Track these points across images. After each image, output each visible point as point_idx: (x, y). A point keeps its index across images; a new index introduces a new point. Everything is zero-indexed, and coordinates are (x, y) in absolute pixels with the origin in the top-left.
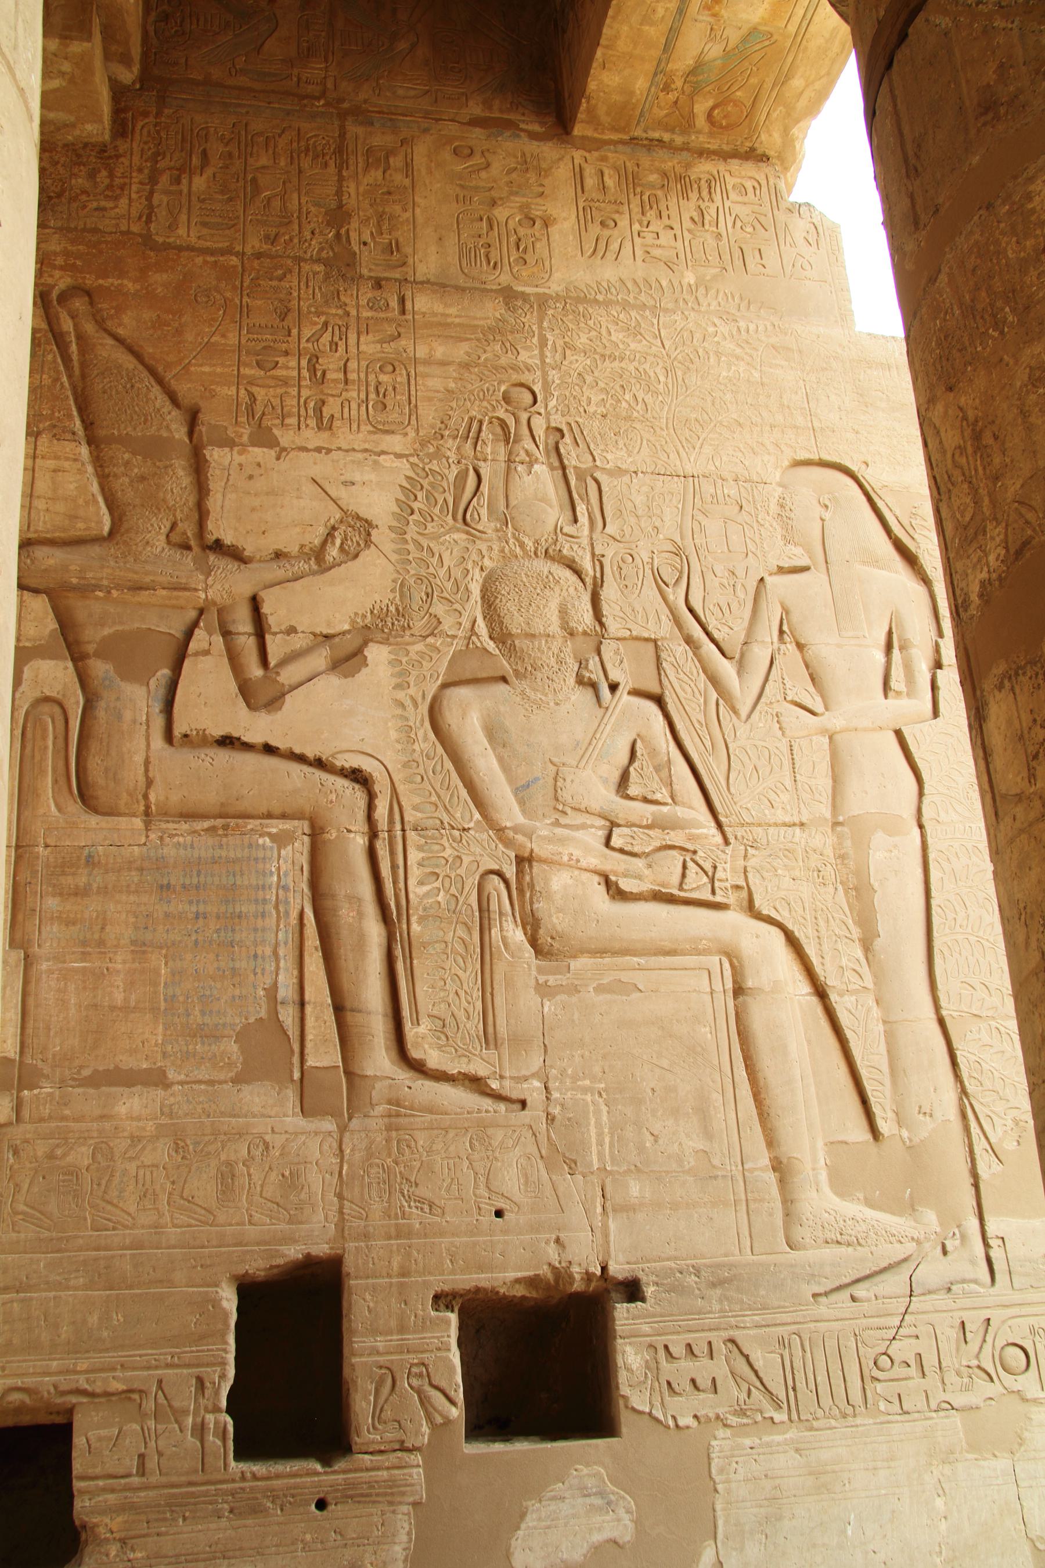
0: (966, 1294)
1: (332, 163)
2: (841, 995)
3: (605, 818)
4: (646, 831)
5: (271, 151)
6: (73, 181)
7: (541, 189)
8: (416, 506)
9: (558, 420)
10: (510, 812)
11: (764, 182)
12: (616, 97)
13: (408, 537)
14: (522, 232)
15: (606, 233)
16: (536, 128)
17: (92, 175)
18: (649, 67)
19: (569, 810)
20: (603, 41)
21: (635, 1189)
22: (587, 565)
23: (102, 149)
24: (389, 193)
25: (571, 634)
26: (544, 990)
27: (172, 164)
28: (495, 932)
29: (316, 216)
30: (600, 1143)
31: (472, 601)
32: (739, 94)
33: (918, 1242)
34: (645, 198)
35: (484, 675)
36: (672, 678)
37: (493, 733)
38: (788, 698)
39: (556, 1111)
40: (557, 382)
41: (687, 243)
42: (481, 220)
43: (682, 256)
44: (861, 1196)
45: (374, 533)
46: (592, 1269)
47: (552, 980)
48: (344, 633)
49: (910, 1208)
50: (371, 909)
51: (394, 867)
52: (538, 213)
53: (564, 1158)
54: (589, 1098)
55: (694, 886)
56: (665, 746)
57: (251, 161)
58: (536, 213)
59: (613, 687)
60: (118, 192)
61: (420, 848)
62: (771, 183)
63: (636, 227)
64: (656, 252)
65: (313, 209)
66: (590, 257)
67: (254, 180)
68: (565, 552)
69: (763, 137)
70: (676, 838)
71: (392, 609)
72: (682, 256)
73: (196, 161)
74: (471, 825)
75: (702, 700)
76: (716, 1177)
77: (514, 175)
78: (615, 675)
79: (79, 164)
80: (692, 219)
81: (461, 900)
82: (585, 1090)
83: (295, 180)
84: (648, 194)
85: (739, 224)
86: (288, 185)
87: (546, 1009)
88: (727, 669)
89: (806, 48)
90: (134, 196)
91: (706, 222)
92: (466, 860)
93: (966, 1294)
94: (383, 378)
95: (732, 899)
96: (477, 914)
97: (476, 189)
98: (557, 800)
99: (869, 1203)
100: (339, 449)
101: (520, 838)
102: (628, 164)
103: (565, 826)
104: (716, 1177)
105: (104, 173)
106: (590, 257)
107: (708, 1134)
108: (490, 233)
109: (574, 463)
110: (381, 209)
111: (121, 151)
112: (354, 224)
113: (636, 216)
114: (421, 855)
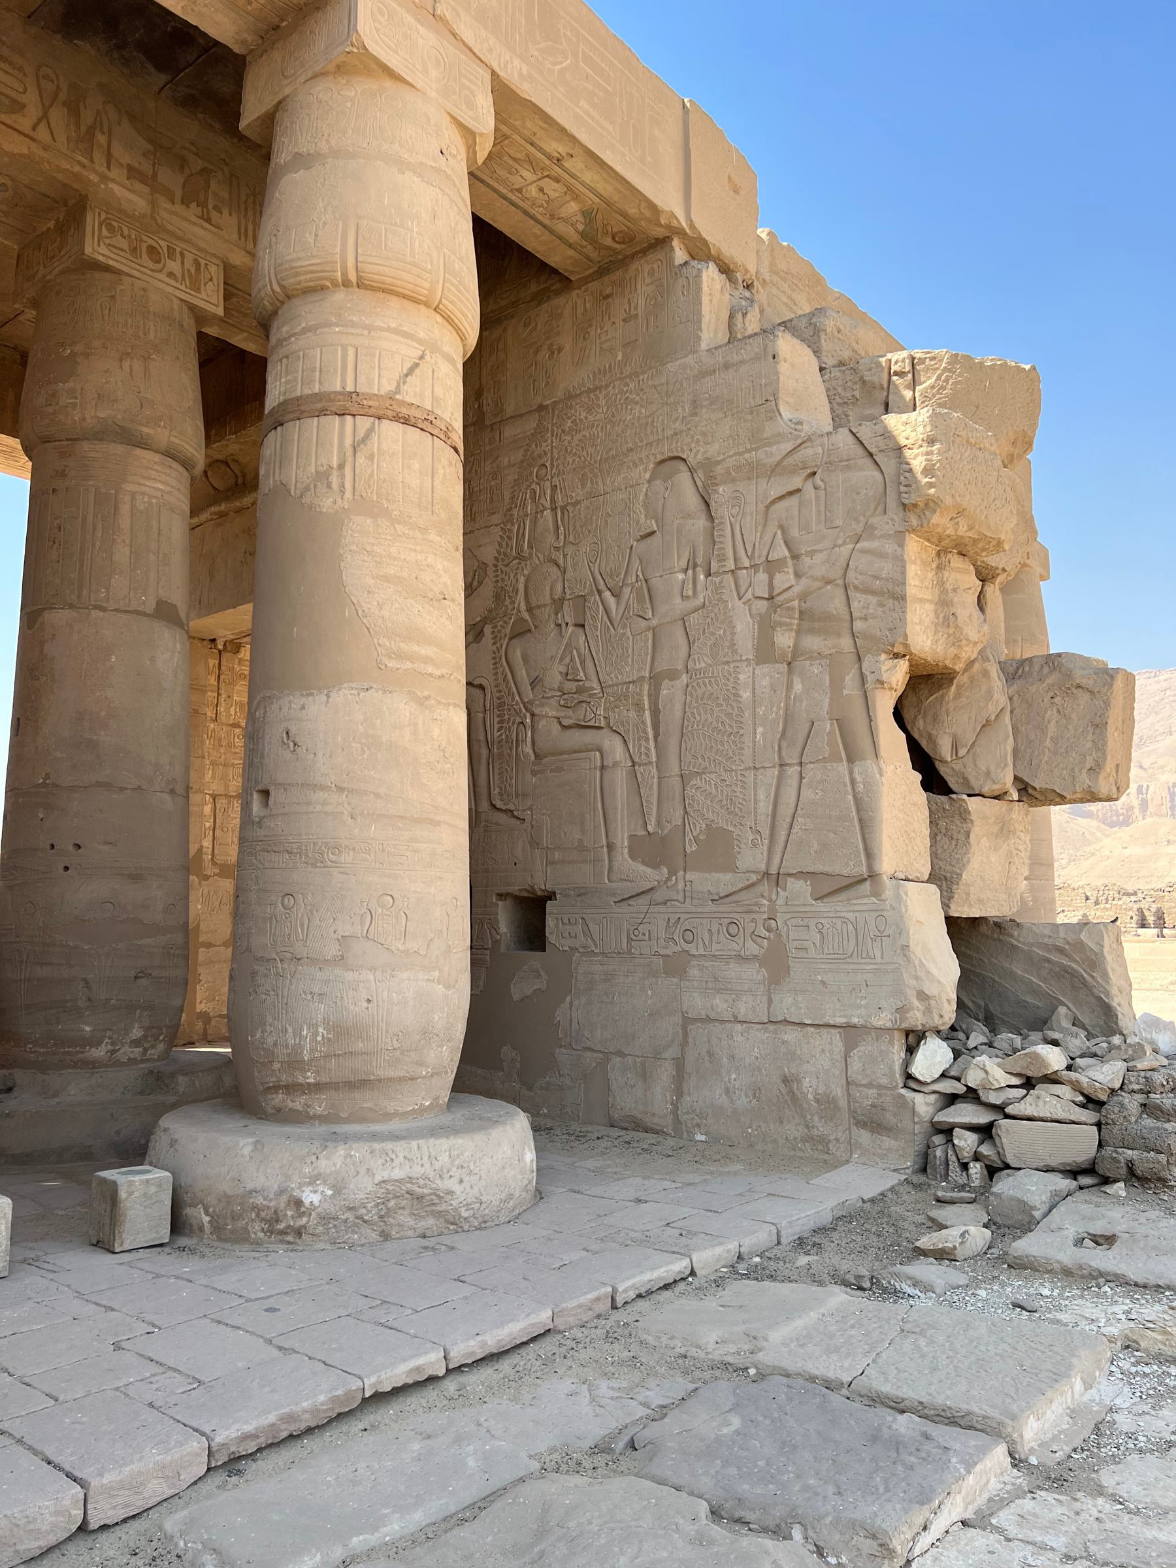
0: (673, 906)
9: (556, 481)
10: (529, 695)
18: (563, 246)
22: (561, 562)
26: (534, 773)
49: (655, 866)
50: (483, 744)
53: (534, 843)
78: (568, 619)
82: (544, 814)
93: (673, 906)
94: (493, 483)
107: (583, 832)
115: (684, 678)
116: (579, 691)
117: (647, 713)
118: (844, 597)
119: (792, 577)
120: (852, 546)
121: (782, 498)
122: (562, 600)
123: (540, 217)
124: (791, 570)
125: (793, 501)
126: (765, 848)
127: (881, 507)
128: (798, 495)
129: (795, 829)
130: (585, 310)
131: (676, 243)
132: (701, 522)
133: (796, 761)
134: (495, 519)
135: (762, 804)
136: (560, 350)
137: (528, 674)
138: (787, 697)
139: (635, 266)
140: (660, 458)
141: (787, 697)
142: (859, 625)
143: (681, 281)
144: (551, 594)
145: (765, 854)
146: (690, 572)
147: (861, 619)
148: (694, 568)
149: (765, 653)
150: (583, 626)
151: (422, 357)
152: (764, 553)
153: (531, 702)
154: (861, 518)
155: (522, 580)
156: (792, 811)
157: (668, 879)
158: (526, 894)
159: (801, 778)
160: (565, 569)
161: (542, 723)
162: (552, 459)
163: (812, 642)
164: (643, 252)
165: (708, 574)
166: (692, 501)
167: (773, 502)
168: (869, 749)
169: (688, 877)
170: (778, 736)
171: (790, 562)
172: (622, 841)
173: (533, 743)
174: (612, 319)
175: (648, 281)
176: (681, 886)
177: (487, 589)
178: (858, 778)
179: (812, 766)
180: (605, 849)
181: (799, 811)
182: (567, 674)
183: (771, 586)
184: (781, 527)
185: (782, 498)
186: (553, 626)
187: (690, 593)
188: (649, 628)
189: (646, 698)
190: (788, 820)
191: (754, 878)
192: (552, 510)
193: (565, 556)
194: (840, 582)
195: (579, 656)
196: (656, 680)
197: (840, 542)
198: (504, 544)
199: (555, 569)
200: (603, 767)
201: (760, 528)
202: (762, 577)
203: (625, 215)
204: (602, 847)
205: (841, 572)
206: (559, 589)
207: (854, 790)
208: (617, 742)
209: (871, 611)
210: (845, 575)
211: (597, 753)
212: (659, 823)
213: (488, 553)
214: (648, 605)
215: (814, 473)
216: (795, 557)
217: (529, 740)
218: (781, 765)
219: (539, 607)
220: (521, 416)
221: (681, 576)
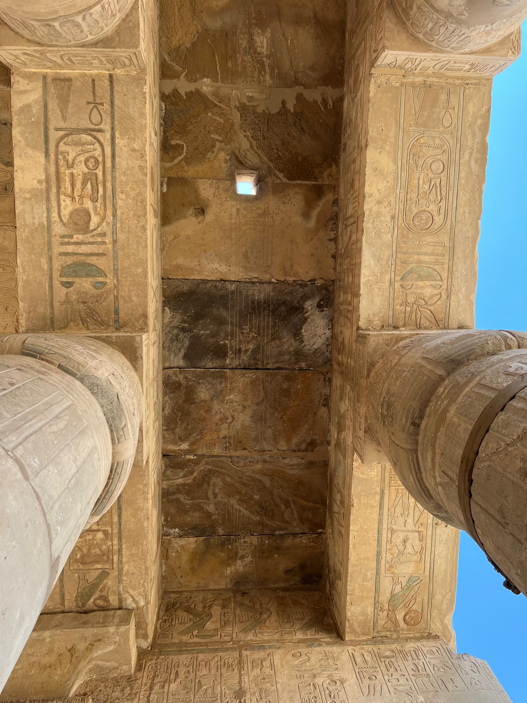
5: (208, 668)
6: (113, 694)
7: (336, 666)
11: (441, 648)
12: (360, 618)
14: (331, 688)
15: (373, 682)
17: (122, 690)
18: (372, 601)
23: (129, 678)
24: (264, 679)
27: (161, 680)
29: (229, 695)
32: (414, 607)
34: (387, 663)
41: (414, 682)
42: (310, 685)
43: (413, 688)
52: (337, 678)
57: (198, 673)
58: (336, 678)
60: (134, 696)
62: (444, 647)
63: (386, 677)
64: (400, 688)
65: (227, 691)
66: (367, 696)
67: (199, 681)
72: (413, 688)
73: (173, 677)
77: (322, 662)
79: (117, 686)
83: (219, 679)
84: (387, 661)
85: (436, 668)
86: (215, 682)
89: (436, 581)
90: (141, 697)
91: (420, 670)
97: (305, 670)
102: (374, 649)
105: (128, 688)
106: (367, 696)
108: (315, 691)
110: (261, 687)
111: (138, 677)
112: (248, 696)
113: (385, 672)
123: (383, 562)
203: (431, 597)
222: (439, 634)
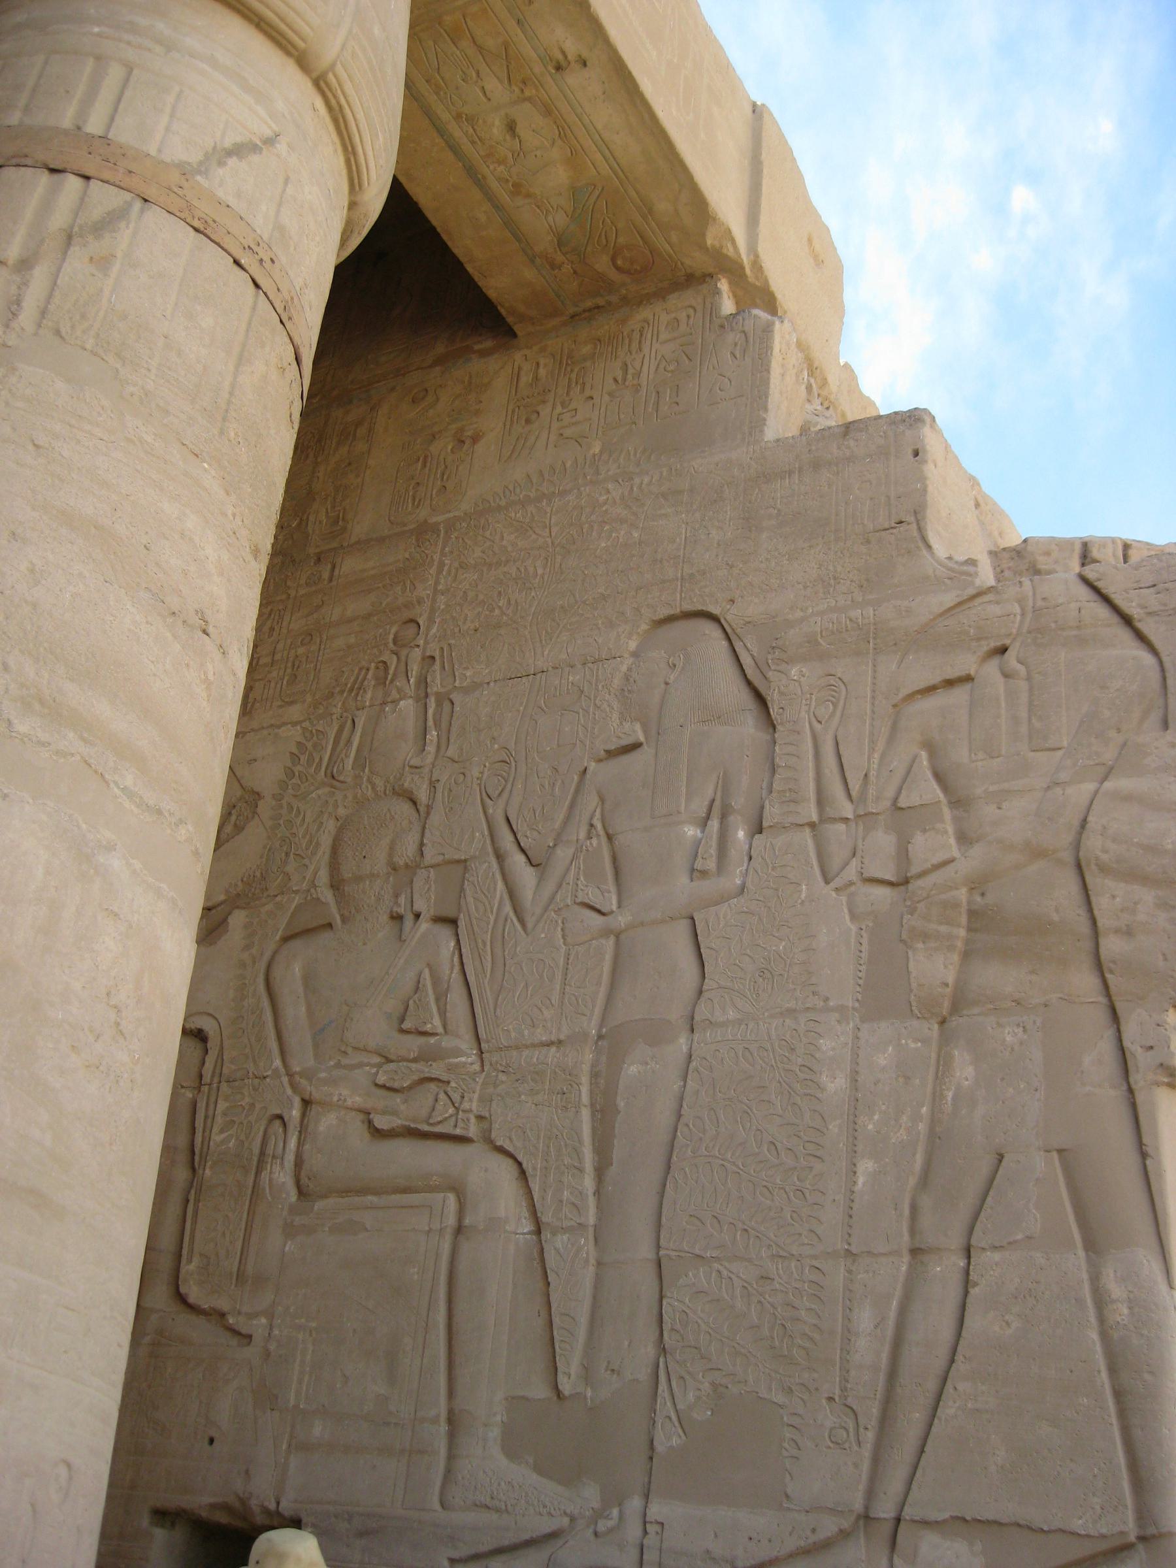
1: (311, 455)
2: (554, 1234)
3: (380, 1055)
4: (409, 1064)
8: (297, 769)
9: (433, 649)
13: (284, 802)
16: (489, 344)
19: (350, 1050)
20: (463, 259)
21: (318, 1430)
22: (422, 796)
25: (395, 869)
26: (289, 1231)
28: (265, 1175)
30: (300, 1382)
31: (320, 853)
33: (573, 1519)
35: (315, 924)
36: (470, 900)
37: (308, 979)
38: (578, 900)
39: (272, 1347)
40: (442, 607)
44: (531, 1461)
45: (260, 803)
46: (266, 1504)
47: (298, 1220)
48: (220, 904)
51: (206, 1117)
54: (300, 1336)
55: (439, 1119)
56: (448, 972)
59: (417, 916)
61: (226, 1099)
63: (559, 409)
64: (568, 432)
68: (406, 785)
69: (687, 262)
70: (436, 1069)
71: (258, 874)
74: (269, 1073)
75: (492, 919)
76: (387, 1424)
78: (420, 905)
80: (615, 380)
81: (246, 1145)
87: (287, 1249)
88: (526, 876)
92: (258, 1106)
94: (301, 651)
95: (473, 1131)
96: (255, 1159)
98: (342, 1040)
99: (538, 1469)
100: (253, 730)
101: (304, 1082)
103: (345, 1067)
104: (387, 1424)
109: (435, 689)
114: (227, 1104)
115: (683, 1041)
116: (424, 1057)
117: (586, 1114)
118: (1074, 887)
119: (952, 841)
120: (1091, 787)
121: (931, 689)
122: (412, 868)
123: (494, 185)
124: (950, 829)
125: (960, 694)
126: (867, 1452)
127: (1155, 717)
128: (968, 687)
129: (948, 1409)
130: (536, 378)
131: (724, 285)
132: (749, 727)
133: (955, 1241)
134: (295, 712)
135: (862, 1343)
136: (475, 439)
137: (310, 1013)
138: (937, 1097)
139: (645, 313)
140: (663, 612)
141: (937, 1097)
142: (1112, 946)
143: (730, 337)
144: (390, 856)
145: (866, 1466)
146: (714, 824)
147: (1117, 931)
148: (723, 817)
149: (883, 995)
150: (453, 922)
151: (270, 141)
152: (890, 793)
153: (309, 1075)
154: (1112, 733)
155: (331, 826)
156: (940, 1363)
157: (598, 1515)
158: (223, 1518)
159: (967, 1283)
160: (429, 808)
161: (326, 1123)
162: (433, 610)
163: (1000, 977)
164: (661, 295)
165: (758, 829)
166: (727, 688)
167: (911, 697)
168: (1144, 1225)
169: (656, 1510)
170: (912, 1181)
171: (947, 812)
172: (488, 1403)
173: (299, 1163)
174: (588, 393)
175: (664, 336)
176: (633, 1531)
177: (254, 837)
178: (1116, 1290)
179: (997, 1256)
180: (443, 1428)
181: (960, 1366)
182: (402, 1020)
183: (903, 854)
184: (930, 747)
185: (931, 689)
186: (385, 918)
187: (711, 865)
188: (606, 932)
189: (585, 1079)
190: (932, 1385)
191: (829, 1526)
192: (417, 700)
193: (433, 785)
194: (1068, 856)
195: (436, 981)
196: (613, 1043)
197: (1063, 776)
198: (304, 759)
199: (405, 808)
200: (459, 1230)
201: (881, 745)
202: (883, 841)
204: (435, 1420)
205: (1067, 838)
206: (407, 849)
207: (1101, 1320)
208: (504, 1171)
209: (1141, 917)
210: (1077, 846)
211: (451, 1198)
212: (587, 1374)
213: (267, 777)
214: (613, 889)
215: (1003, 650)
216: (958, 802)
217: (290, 1157)
218: (915, 1252)
219: (358, 879)
220: (381, 540)
221: (691, 831)
222: (711, 270)
